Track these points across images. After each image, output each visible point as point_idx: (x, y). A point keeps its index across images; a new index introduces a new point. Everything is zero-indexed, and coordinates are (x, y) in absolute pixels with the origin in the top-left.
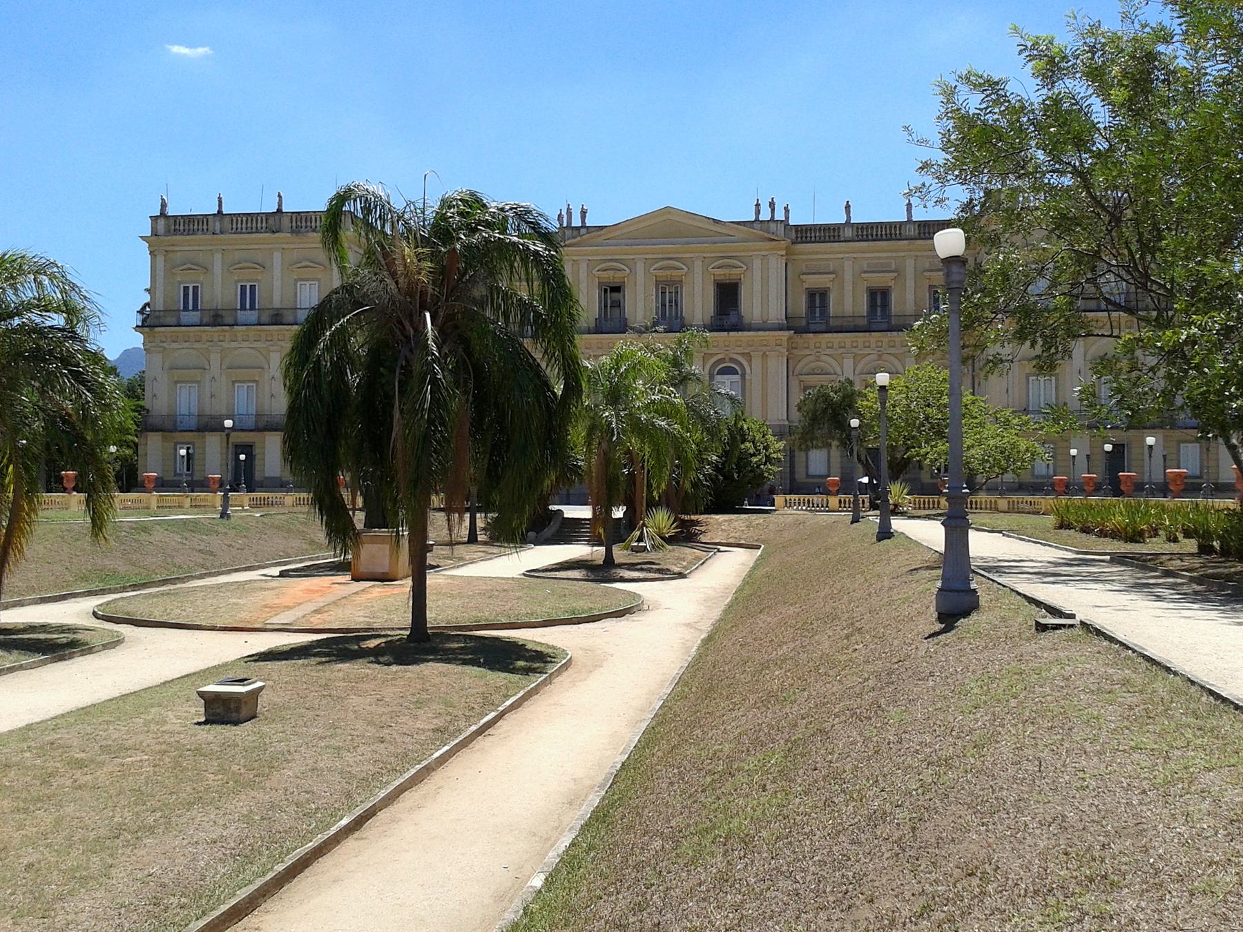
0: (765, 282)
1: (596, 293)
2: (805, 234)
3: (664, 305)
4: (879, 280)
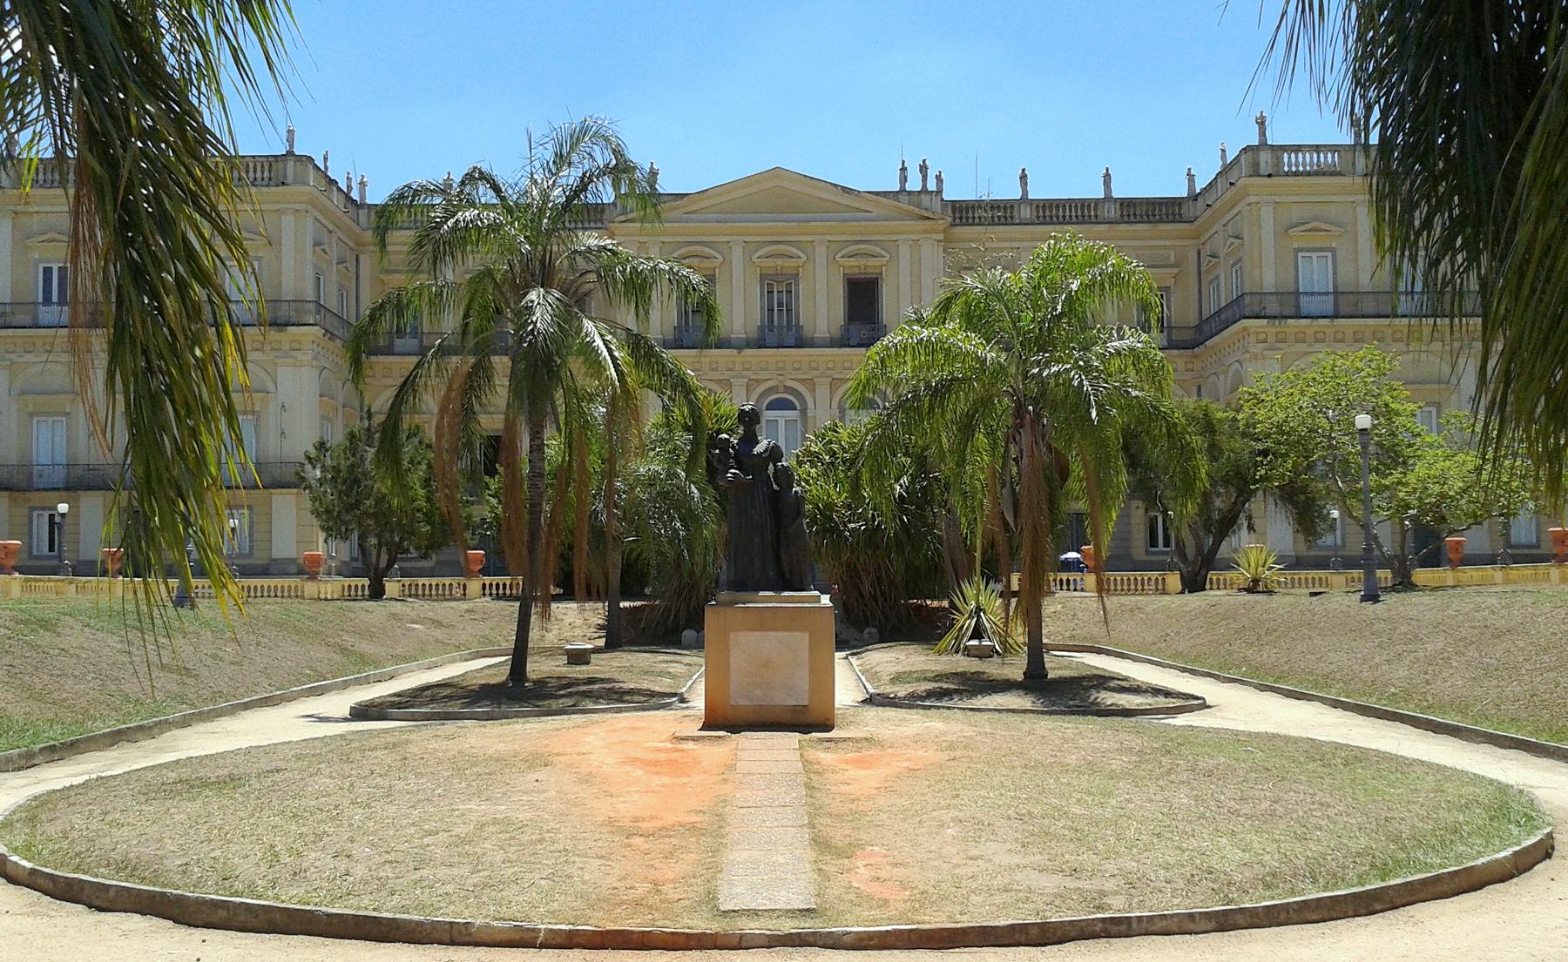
2: (964, 212)
3: (771, 310)
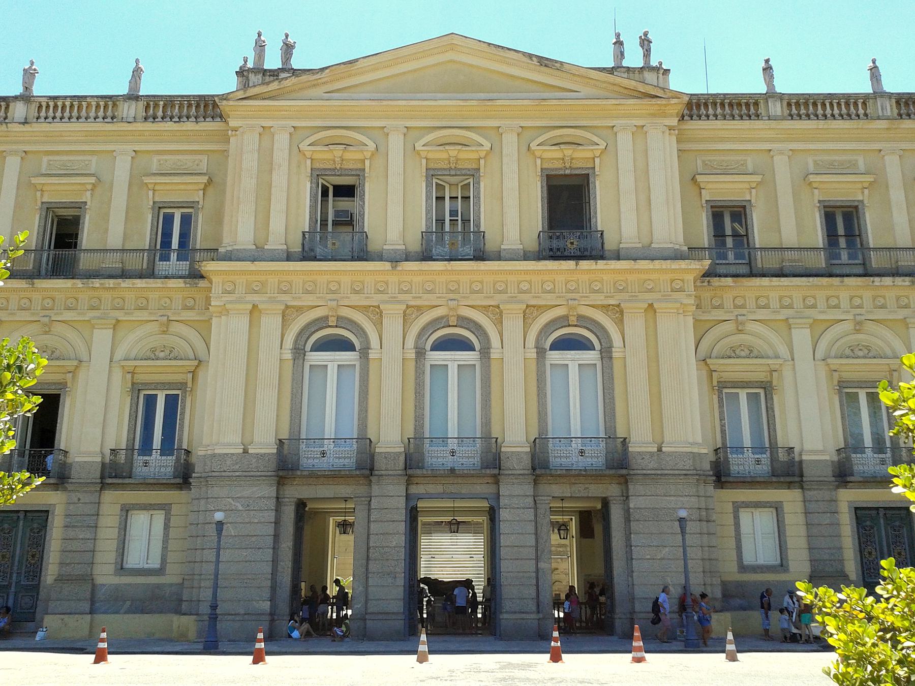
0: (643, 174)
1: (306, 191)
4: (843, 189)
